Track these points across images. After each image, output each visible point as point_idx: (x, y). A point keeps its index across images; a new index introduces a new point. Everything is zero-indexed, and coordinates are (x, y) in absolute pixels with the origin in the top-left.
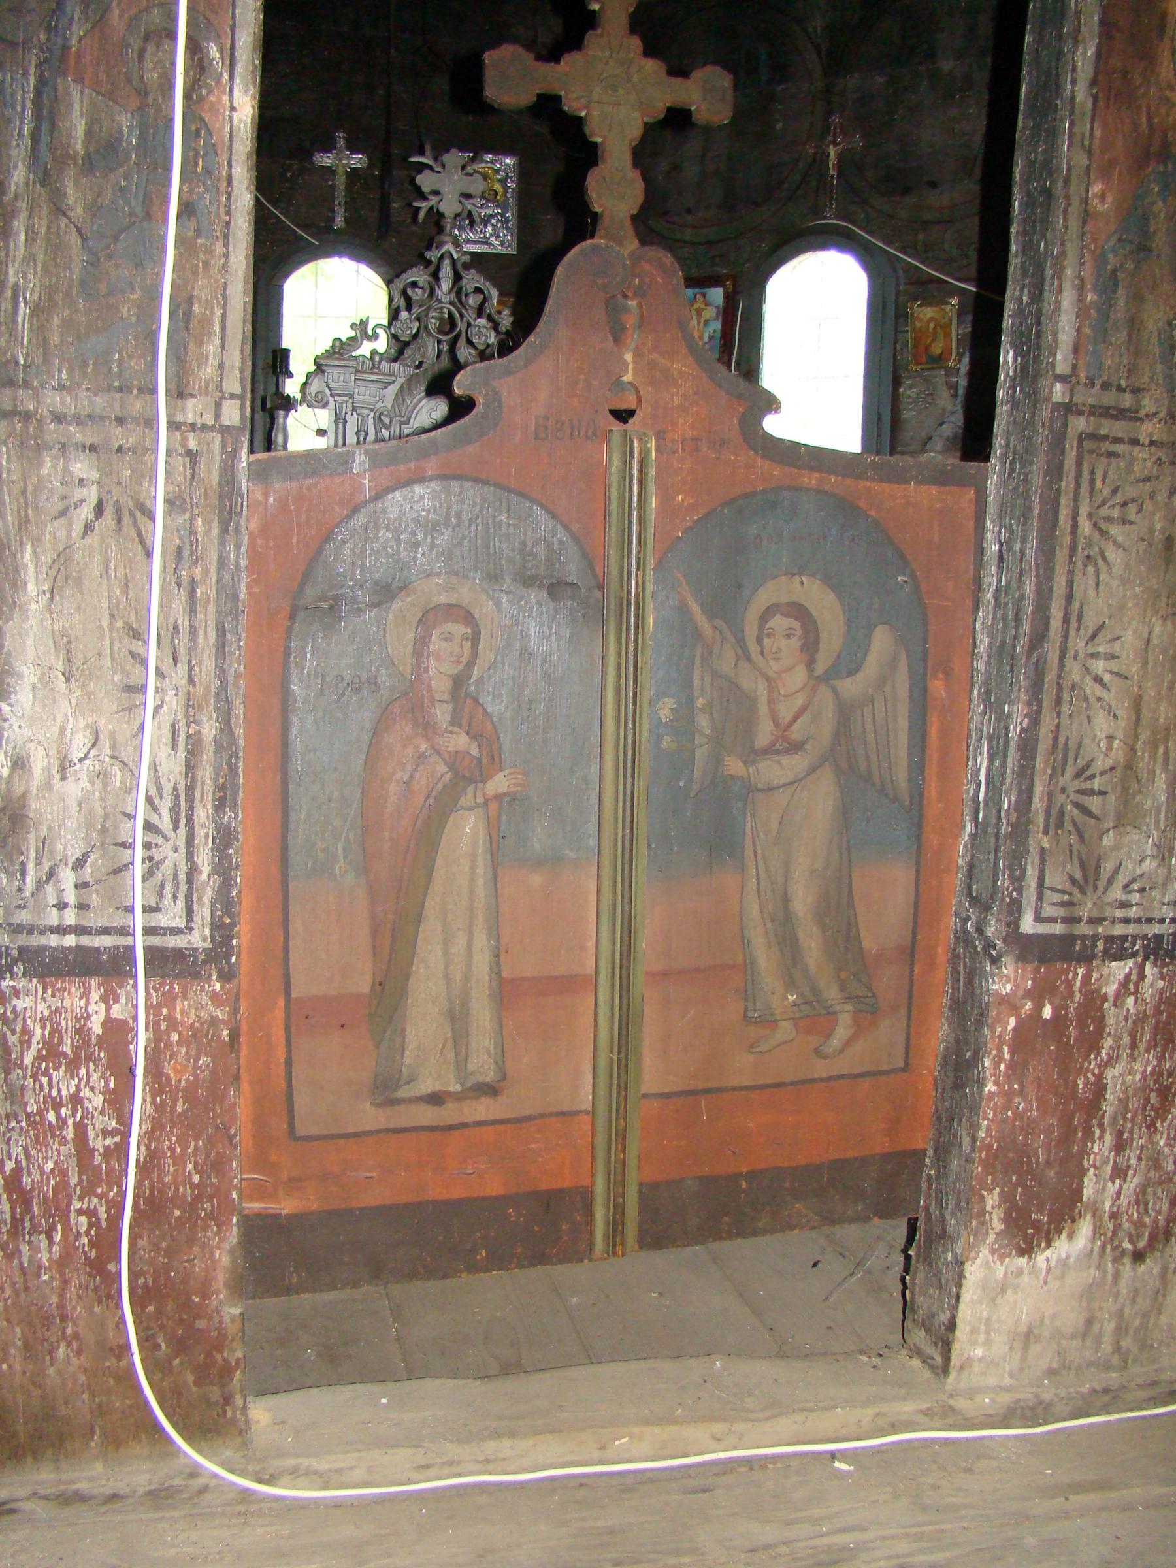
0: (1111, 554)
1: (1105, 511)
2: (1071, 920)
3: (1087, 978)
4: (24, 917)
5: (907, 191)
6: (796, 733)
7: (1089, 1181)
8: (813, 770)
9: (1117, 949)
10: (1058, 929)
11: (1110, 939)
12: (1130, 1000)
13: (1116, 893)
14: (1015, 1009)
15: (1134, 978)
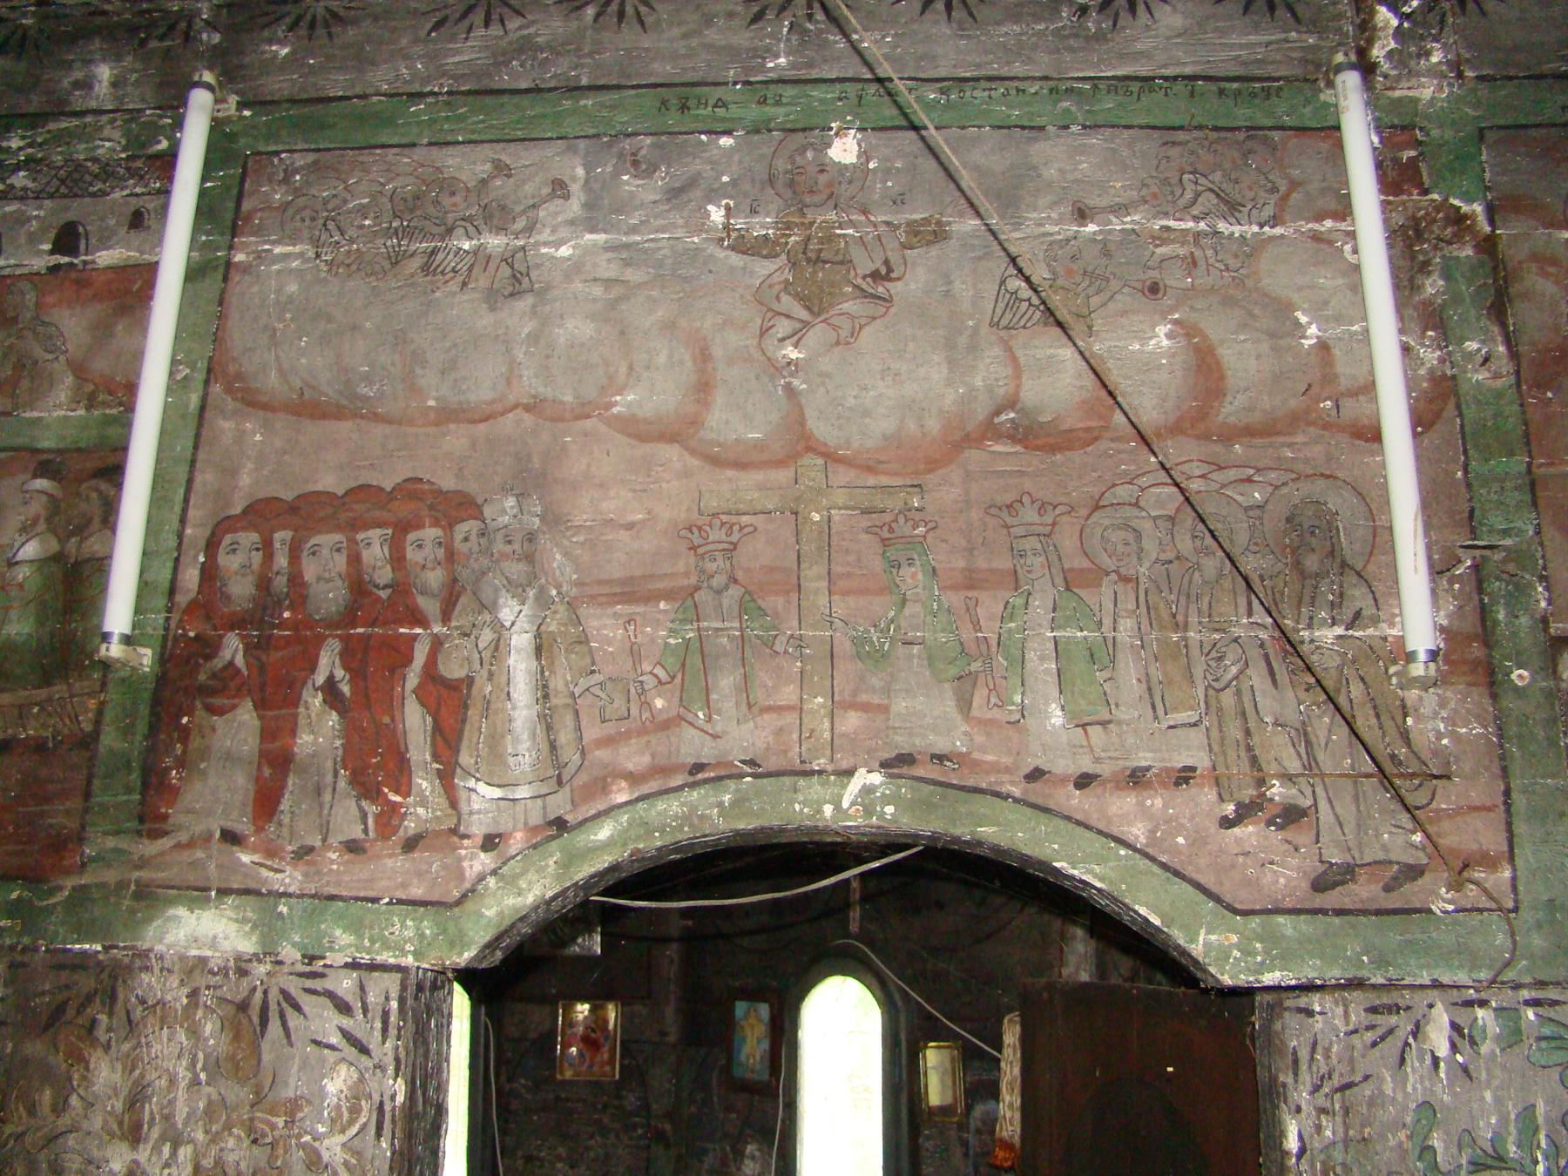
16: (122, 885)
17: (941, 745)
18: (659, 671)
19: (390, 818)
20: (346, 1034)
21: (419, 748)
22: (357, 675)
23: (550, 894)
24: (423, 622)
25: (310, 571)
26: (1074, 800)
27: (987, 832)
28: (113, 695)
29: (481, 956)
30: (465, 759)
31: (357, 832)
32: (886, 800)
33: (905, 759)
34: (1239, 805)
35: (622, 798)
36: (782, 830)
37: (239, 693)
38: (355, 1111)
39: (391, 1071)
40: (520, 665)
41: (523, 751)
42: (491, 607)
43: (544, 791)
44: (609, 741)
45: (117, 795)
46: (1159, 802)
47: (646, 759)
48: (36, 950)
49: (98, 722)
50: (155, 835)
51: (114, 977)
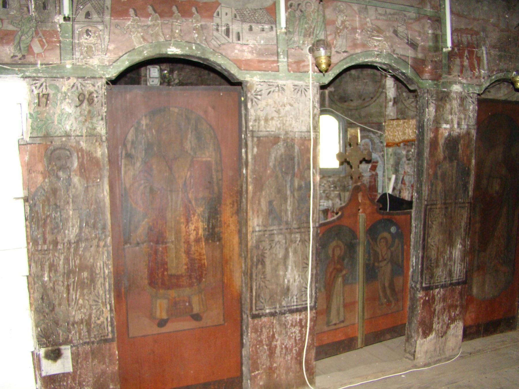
4: (289, 305)
5: (345, 101)
6: (385, 258)
9: (437, 287)
13: (436, 278)
19: (474, 74)
21: (476, 66)
24: (475, 48)
25: (463, 40)
40: (485, 55)
41: (486, 67)
42: (481, 47)
45: (445, 69)
50: (450, 75)
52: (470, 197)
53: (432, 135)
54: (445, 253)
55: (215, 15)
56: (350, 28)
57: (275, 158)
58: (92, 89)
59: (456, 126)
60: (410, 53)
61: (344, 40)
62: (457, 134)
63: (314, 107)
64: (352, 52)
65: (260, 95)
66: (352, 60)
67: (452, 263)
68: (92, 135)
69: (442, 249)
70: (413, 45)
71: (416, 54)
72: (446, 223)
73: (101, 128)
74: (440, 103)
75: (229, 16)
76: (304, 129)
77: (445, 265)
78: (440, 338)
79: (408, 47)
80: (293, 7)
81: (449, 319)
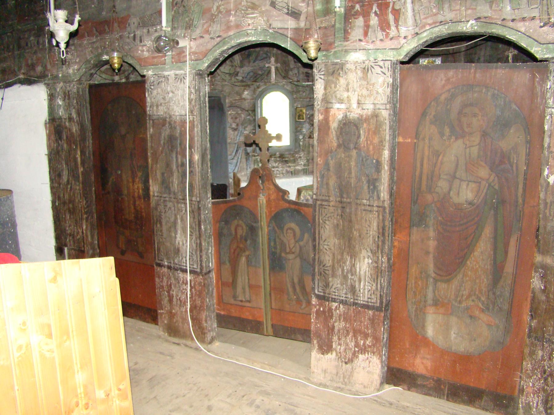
0: (327, 227)
1: (324, 218)
2: (324, 293)
3: (328, 305)
4: (180, 264)
6: (293, 250)
7: (334, 343)
8: (296, 257)
9: (334, 300)
10: (322, 294)
11: (332, 298)
12: (338, 311)
13: (333, 290)
14: (316, 307)
15: (338, 306)
16: (342, 50)
17: (486, 15)
18: (435, 5)
19: (387, 35)
20: (382, 72)
22: (380, 10)
23: (415, 46)
26: (511, 24)
27: (494, 31)
28: (337, 18)
29: (403, 58)
30: (400, 23)
31: (382, 38)
32: (475, 26)
33: (479, 18)
34: (544, 23)
35: (428, 28)
36: (457, 33)
37: (359, 15)
38: (384, 84)
39: (389, 77)
41: (410, 21)
43: (414, 28)
44: (425, 18)
45: (340, 35)
46: (527, 24)
47: (432, 21)
48: (329, 62)
49: (335, 22)
50: (347, 41)
51: (342, 65)
52: (382, 199)
53: (321, 117)
54: (345, 263)
55: (127, 25)
56: (224, 12)
57: (164, 137)
58: (68, 89)
59: (355, 105)
60: (291, 23)
61: (219, 25)
62: (357, 116)
63: (190, 93)
64: (225, 35)
65: (153, 86)
66: (224, 44)
67: (356, 279)
68: (70, 119)
69: (339, 257)
70: (295, 14)
71: (298, 24)
72: (343, 226)
73: (74, 115)
74: (330, 78)
75: (136, 24)
76: (183, 113)
77: (345, 277)
78: (344, 364)
79: (287, 17)
80: (178, 5)
81: (355, 346)
